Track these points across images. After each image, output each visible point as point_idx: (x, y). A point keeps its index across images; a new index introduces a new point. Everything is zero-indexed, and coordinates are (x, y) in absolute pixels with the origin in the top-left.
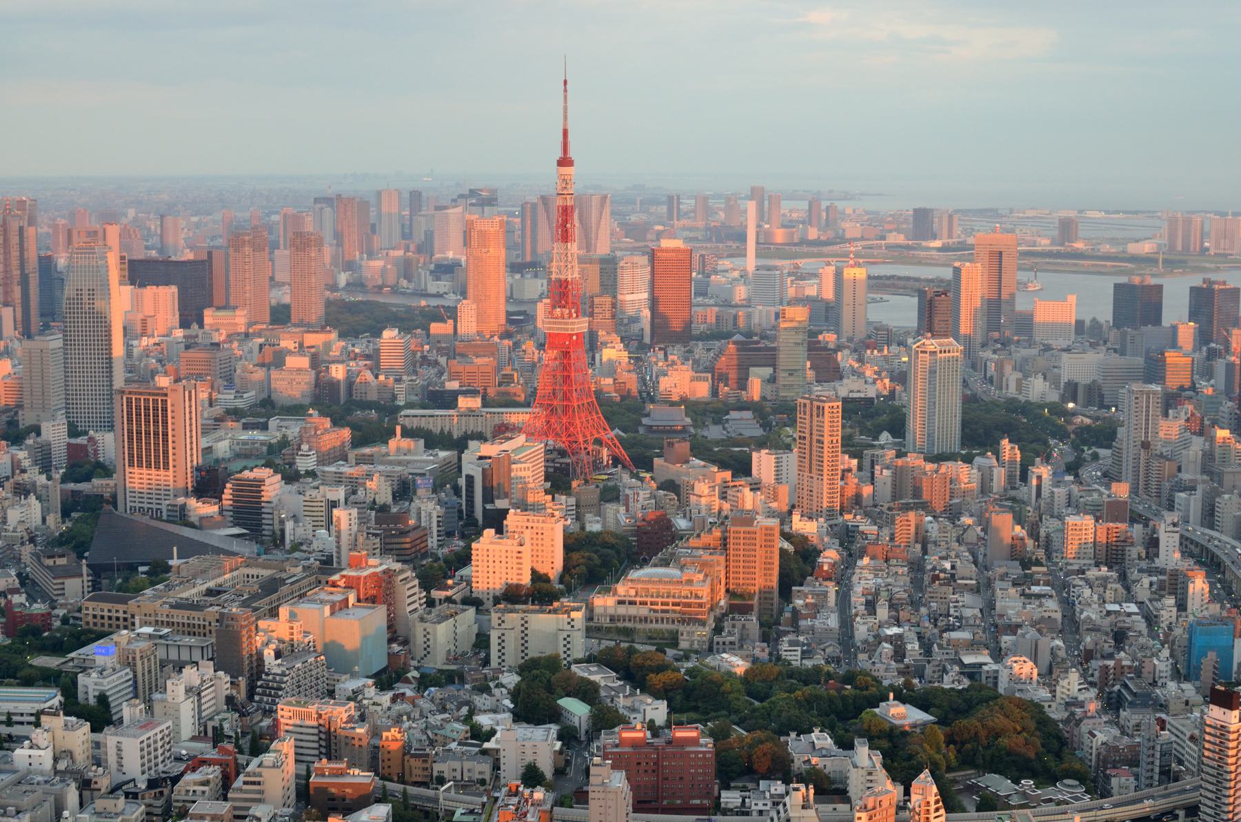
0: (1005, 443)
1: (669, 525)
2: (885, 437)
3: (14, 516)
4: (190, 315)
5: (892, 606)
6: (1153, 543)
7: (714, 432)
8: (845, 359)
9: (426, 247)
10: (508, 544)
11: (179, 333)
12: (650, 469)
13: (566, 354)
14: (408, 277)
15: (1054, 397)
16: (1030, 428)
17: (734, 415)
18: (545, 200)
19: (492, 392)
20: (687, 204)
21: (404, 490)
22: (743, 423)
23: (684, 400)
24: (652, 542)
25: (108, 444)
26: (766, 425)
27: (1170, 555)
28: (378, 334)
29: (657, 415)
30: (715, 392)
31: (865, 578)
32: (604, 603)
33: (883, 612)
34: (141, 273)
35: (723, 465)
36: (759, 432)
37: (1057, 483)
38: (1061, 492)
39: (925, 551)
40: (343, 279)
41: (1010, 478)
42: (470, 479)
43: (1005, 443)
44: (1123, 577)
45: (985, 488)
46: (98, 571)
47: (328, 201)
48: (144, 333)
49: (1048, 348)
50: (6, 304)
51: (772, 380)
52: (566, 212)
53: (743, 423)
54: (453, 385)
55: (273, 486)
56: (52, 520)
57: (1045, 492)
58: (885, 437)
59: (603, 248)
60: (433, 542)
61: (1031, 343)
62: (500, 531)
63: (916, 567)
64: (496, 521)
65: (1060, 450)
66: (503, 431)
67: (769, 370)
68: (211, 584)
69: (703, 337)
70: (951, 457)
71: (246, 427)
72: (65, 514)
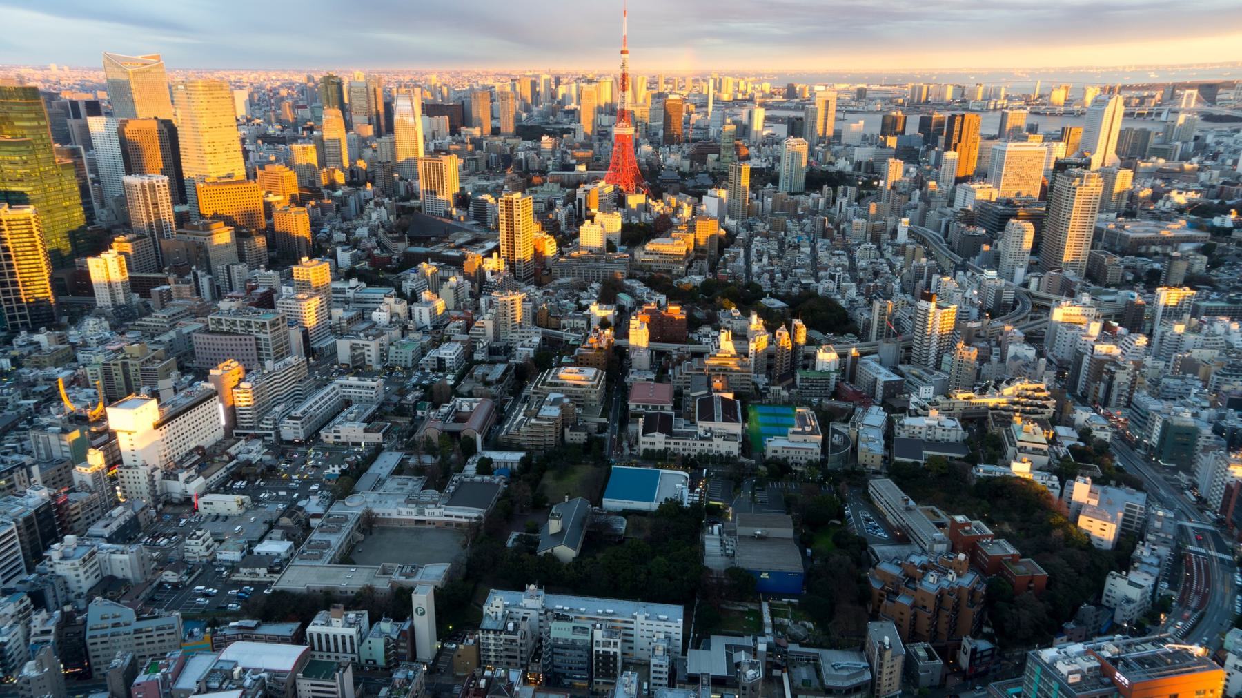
0: (826, 187)
1: (669, 221)
2: (770, 185)
3: (374, 216)
4: (454, 131)
5: (770, 258)
6: (894, 232)
7: (690, 183)
9: (562, 103)
10: (597, 227)
11: (449, 139)
12: (661, 197)
14: (554, 116)
15: (849, 169)
16: (837, 180)
19: (591, 164)
21: (551, 206)
22: (703, 179)
23: (678, 168)
24: (662, 227)
26: (714, 180)
27: (902, 237)
29: (664, 175)
30: (691, 166)
31: (757, 243)
32: (639, 254)
33: (765, 260)
34: (430, 110)
37: (849, 205)
38: (851, 210)
40: (524, 115)
41: (827, 203)
42: (580, 200)
43: (826, 187)
44: (879, 248)
48: (434, 138)
49: (848, 146)
51: (718, 160)
52: (624, 76)
53: (703, 179)
54: (573, 162)
56: (391, 218)
57: (844, 209)
58: (770, 185)
60: (563, 227)
61: (840, 144)
62: (592, 222)
63: (781, 242)
65: (852, 190)
67: (715, 156)
69: (687, 141)
70: (800, 193)
72: (398, 216)
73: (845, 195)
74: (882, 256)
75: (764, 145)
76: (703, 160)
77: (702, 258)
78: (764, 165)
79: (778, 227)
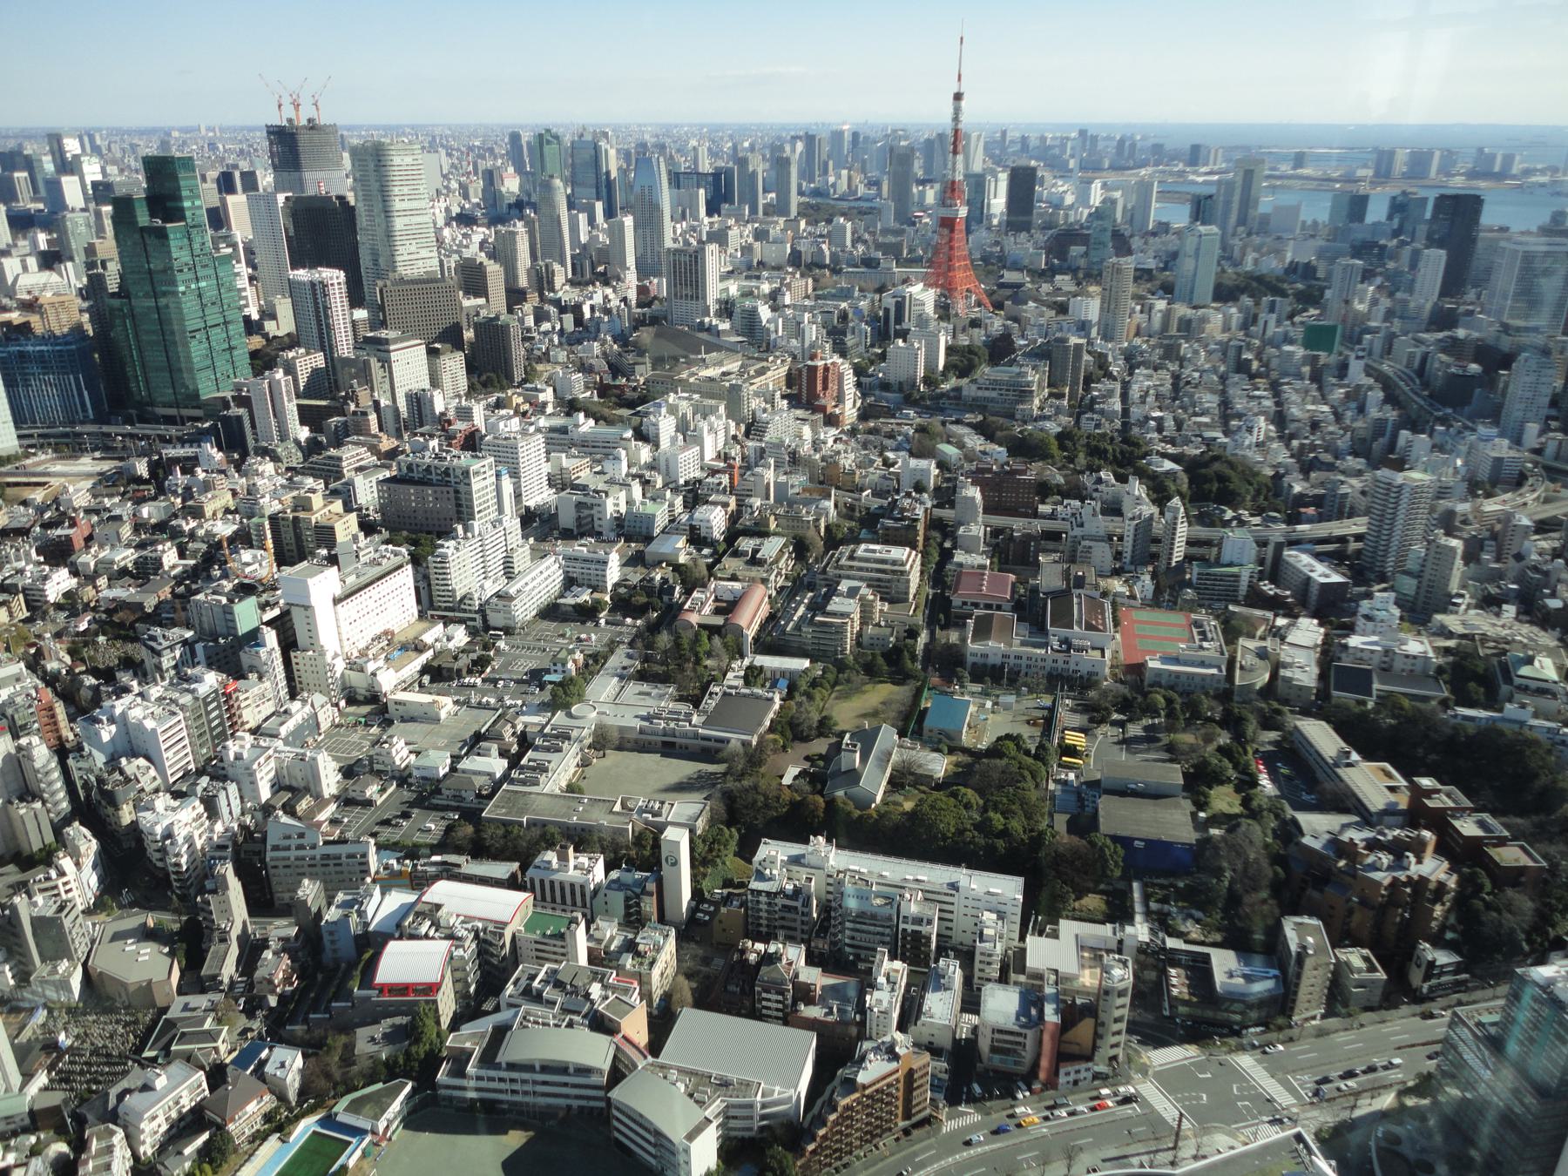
7: (1046, 287)
8: (1136, 243)
11: (706, 220)
13: (952, 231)
17: (1058, 277)
18: (941, 136)
20: (1033, 143)
25: (660, 286)
26: (1078, 284)
28: (829, 221)
29: (1010, 276)
35: (1049, 307)
36: (1073, 288)
39: (1181, 366)
42: (887, 311)
45: (1226, 328)
46: (658, 362)
47: (800, 138)
48: (684, 217)
50: (598, 199)
51: (1086, 254)
52: (956, 131)
54: (880, 255)
55: (765, 313)
59: (977, 167)
63: (1176, 377)
64: (904, 335)
66: (906, 281)
67: (1083, 249)
68: (724, 369)
71: (747, 278)
73: (1272, 309)
74: (1324, 399)
75: (1154, 234)
76: (1063, 255)
77: (1060, 396)
78: (1151, 263)
79: (1171, 352)
